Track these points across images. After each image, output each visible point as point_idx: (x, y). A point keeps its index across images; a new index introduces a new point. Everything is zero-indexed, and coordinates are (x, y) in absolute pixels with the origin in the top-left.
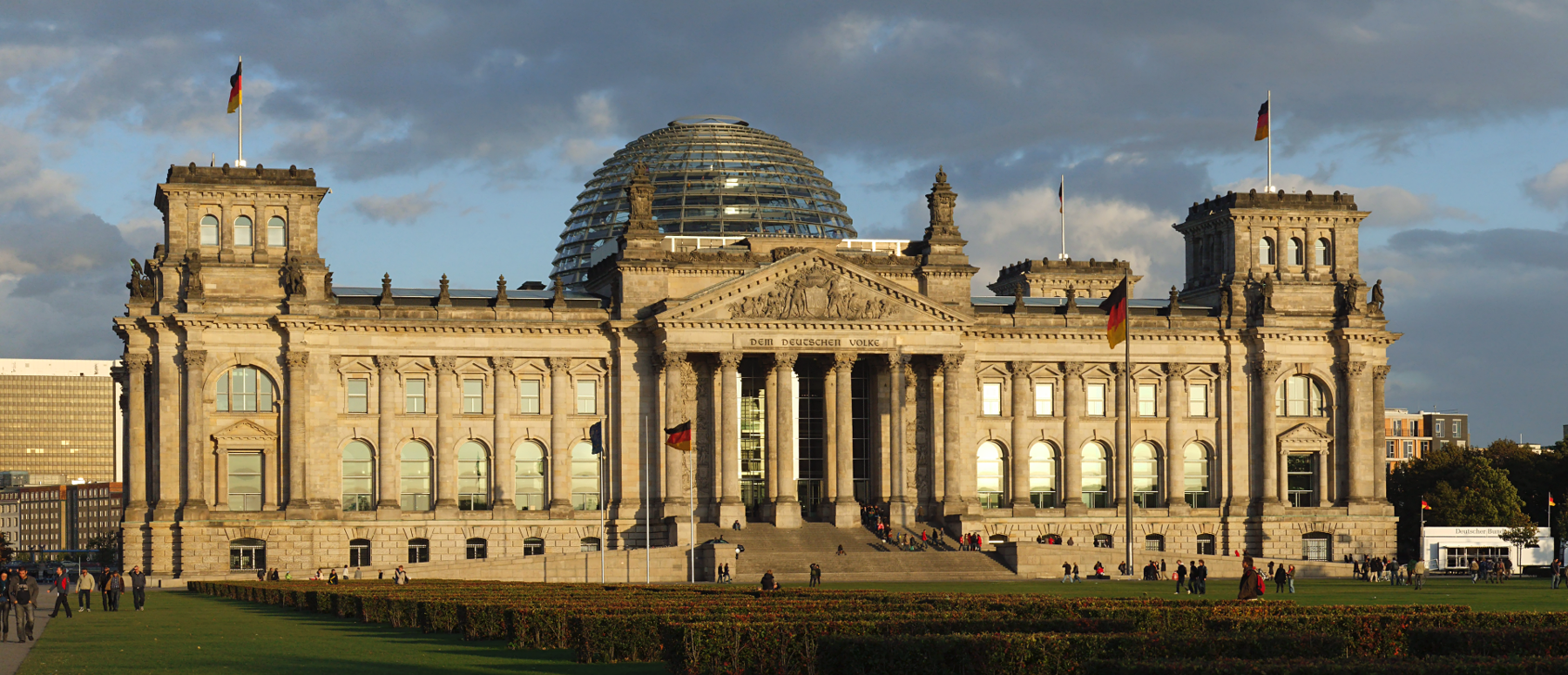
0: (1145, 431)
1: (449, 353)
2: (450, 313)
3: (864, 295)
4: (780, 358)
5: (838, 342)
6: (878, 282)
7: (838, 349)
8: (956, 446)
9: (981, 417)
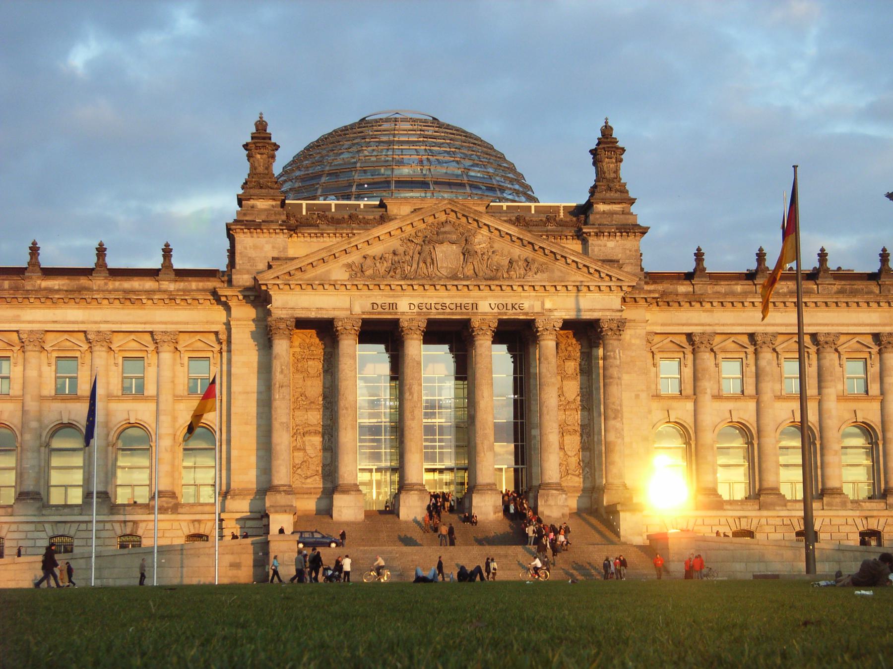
0: (855, 411)
1: (36, 327)
2: (39, 282)
3: (506, 252)
4: (404, 324)
5: (475, 306)
6: (521, 237)
7: (475, 314)
8: (618, 425)
9: (657, 396)
